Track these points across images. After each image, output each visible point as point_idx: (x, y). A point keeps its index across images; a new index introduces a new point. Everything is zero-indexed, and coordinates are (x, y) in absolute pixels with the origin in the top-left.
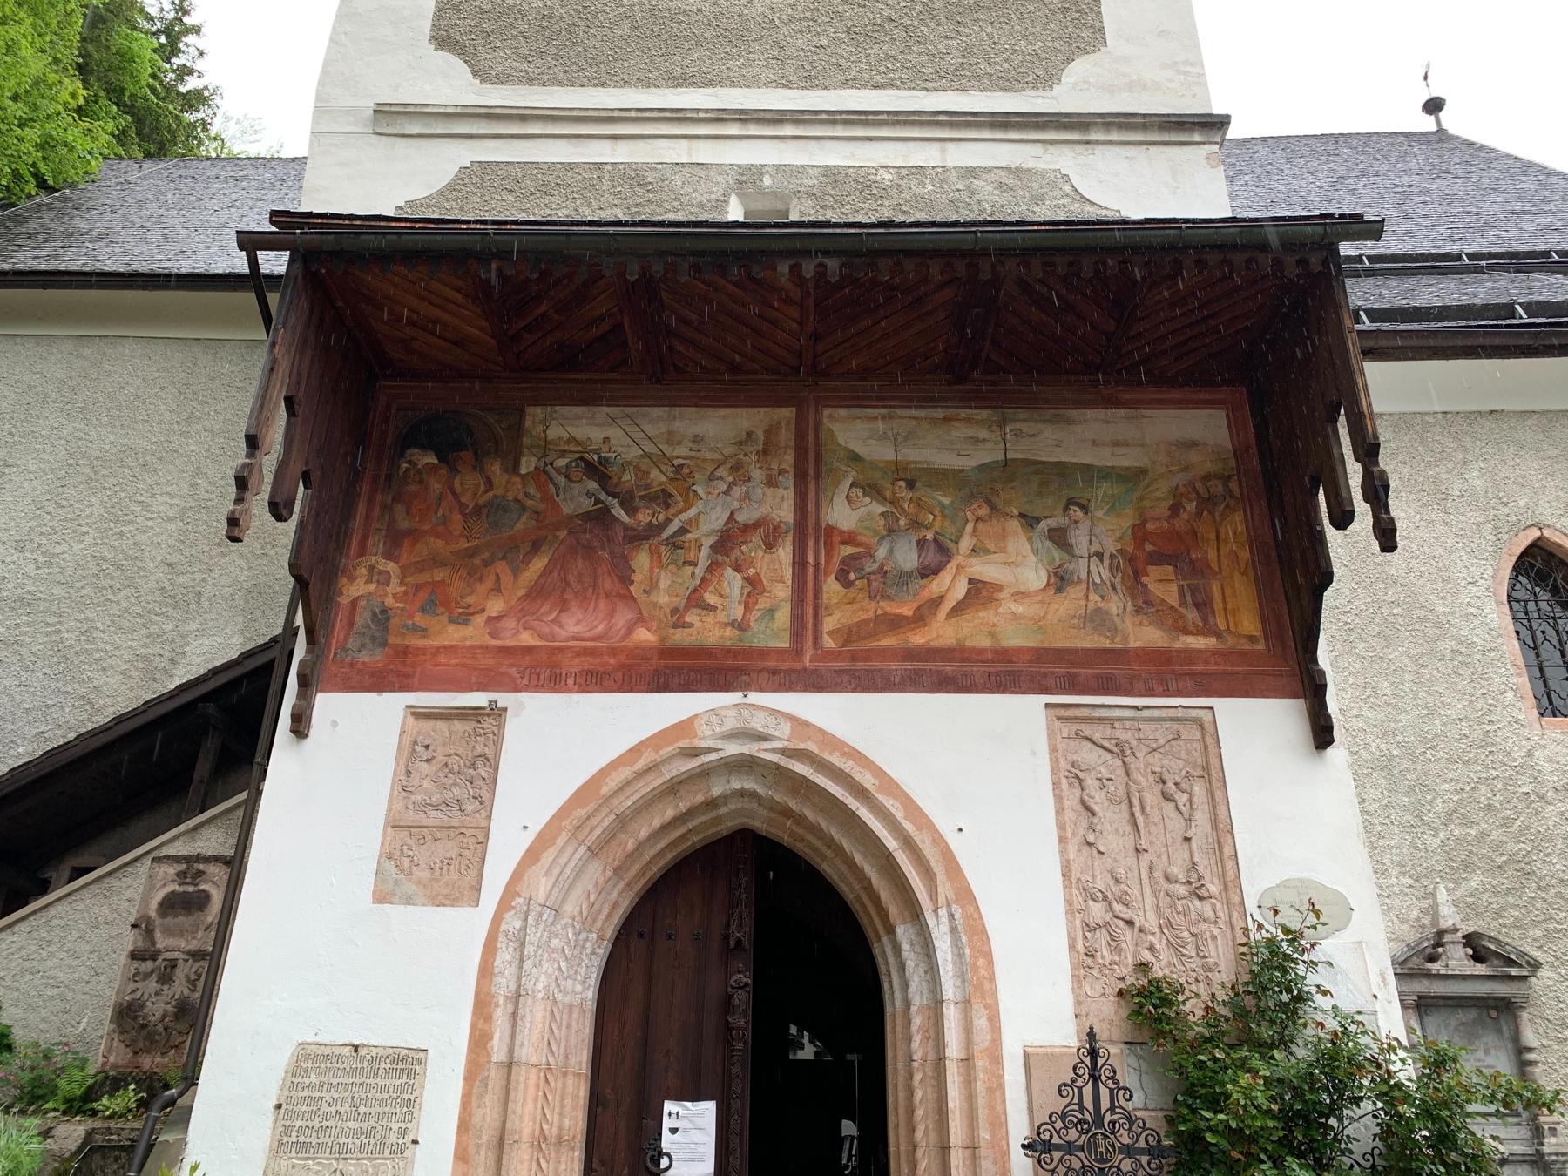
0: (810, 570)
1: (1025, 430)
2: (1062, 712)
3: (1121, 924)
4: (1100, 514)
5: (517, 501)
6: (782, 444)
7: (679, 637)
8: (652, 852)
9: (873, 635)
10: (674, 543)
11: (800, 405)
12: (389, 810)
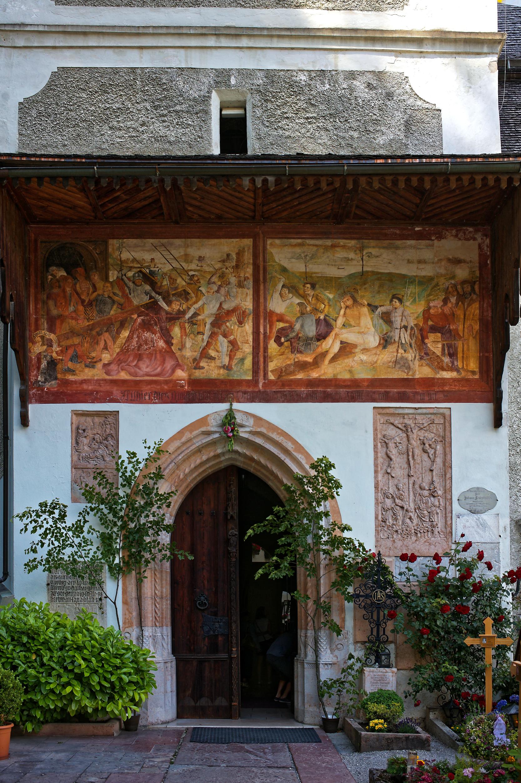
0: (262, 336)
1: (373, 253)
2: (381, 411)
3: (398, 508)
4: (408, 304)
5: (109, 297)
6: (246, 262)
7: (198, 374)
8: (191, 478)
9: (293, 373)
10: (192, 322)
11: (255, 237)
12: (72, 461)
